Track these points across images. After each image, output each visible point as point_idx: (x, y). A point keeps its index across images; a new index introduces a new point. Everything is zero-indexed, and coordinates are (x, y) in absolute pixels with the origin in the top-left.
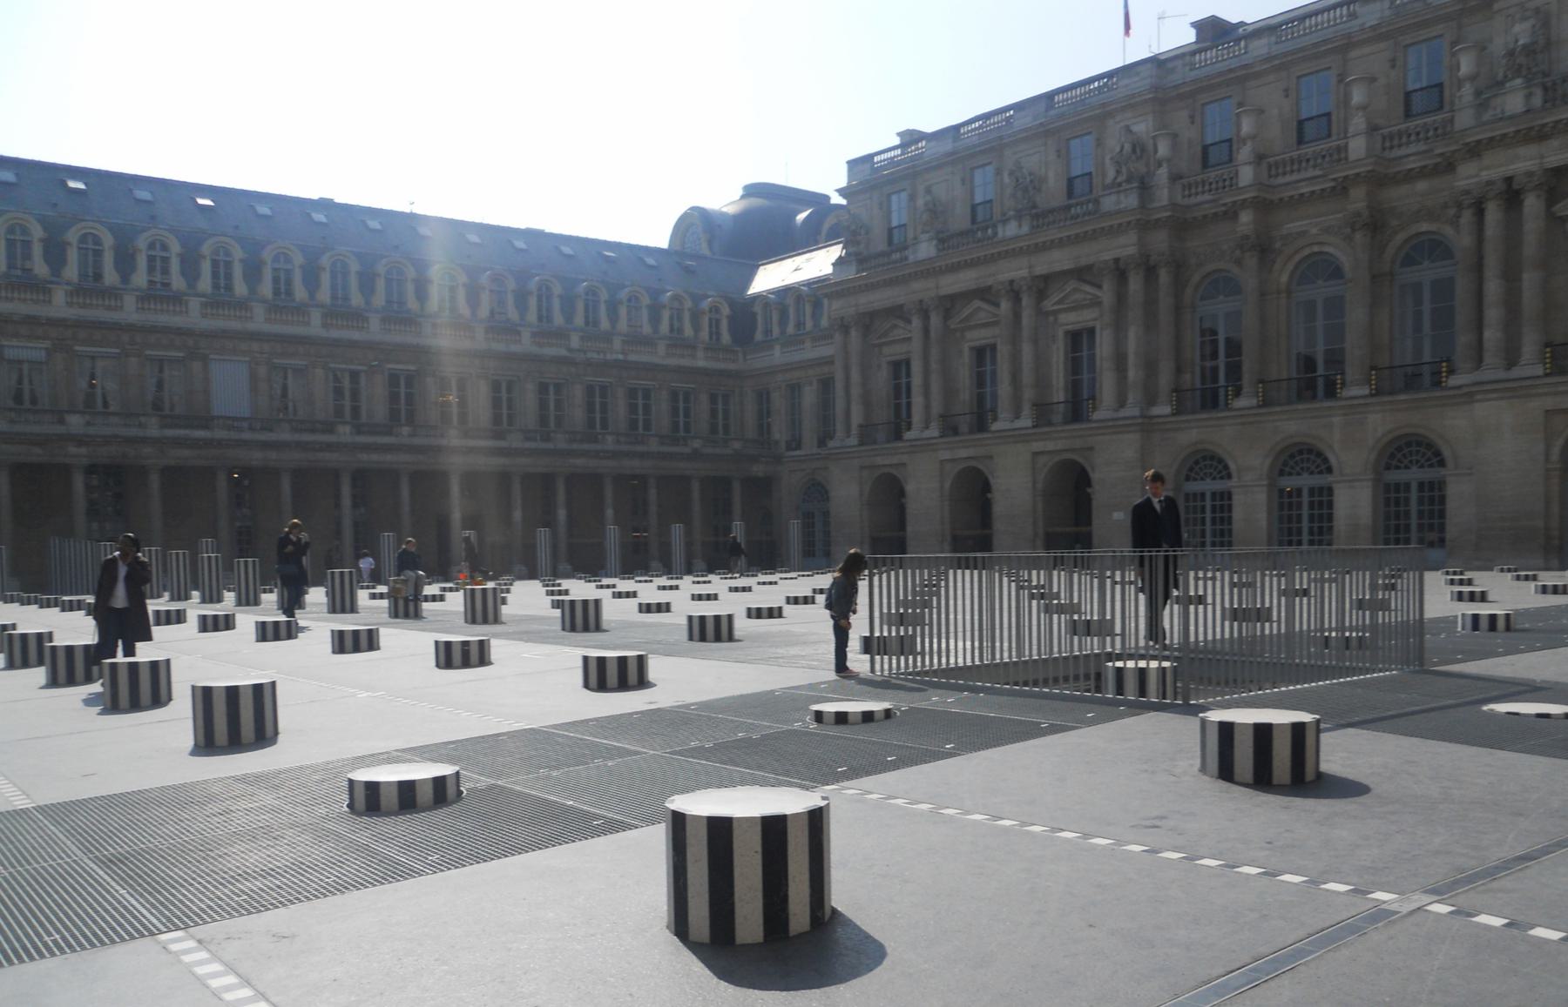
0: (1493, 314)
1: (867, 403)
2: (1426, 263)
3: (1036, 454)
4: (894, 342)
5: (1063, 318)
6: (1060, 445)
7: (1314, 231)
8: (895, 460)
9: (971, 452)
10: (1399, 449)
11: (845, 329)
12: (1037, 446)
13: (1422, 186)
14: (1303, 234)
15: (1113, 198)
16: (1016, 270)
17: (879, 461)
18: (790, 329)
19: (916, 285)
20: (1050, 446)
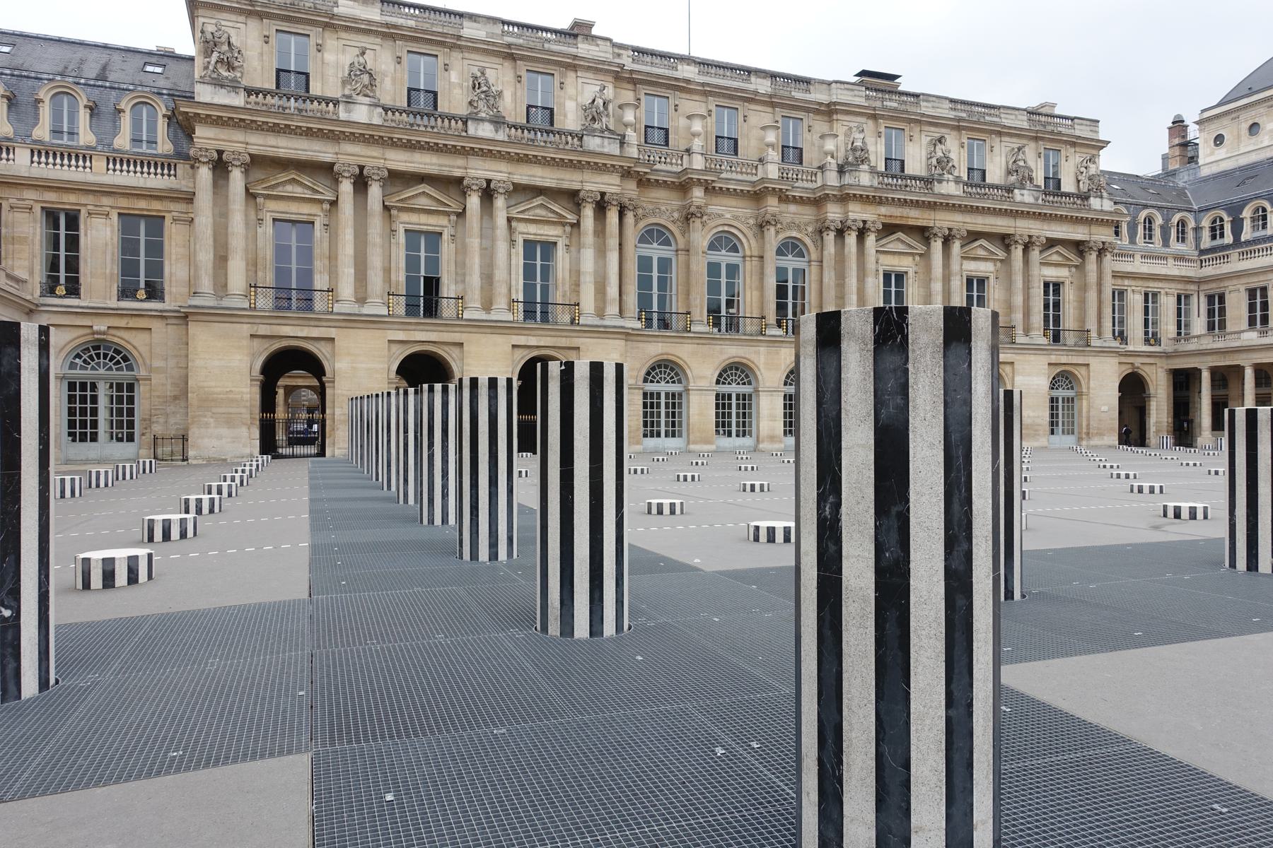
1: (253, 264)
2: (790, 257)
3: (514, 346)
5: (521, 227)
7: (728, 216)
8: (315, 333)
9: (433, 336)
11: (220, 166)
12: (522, 340)
13: (793, 208)
14: (720, 216)
15: (598, 140)
16: (499, 172)
18: (42, 132)
19: (349, 148)
20: (533, 341)
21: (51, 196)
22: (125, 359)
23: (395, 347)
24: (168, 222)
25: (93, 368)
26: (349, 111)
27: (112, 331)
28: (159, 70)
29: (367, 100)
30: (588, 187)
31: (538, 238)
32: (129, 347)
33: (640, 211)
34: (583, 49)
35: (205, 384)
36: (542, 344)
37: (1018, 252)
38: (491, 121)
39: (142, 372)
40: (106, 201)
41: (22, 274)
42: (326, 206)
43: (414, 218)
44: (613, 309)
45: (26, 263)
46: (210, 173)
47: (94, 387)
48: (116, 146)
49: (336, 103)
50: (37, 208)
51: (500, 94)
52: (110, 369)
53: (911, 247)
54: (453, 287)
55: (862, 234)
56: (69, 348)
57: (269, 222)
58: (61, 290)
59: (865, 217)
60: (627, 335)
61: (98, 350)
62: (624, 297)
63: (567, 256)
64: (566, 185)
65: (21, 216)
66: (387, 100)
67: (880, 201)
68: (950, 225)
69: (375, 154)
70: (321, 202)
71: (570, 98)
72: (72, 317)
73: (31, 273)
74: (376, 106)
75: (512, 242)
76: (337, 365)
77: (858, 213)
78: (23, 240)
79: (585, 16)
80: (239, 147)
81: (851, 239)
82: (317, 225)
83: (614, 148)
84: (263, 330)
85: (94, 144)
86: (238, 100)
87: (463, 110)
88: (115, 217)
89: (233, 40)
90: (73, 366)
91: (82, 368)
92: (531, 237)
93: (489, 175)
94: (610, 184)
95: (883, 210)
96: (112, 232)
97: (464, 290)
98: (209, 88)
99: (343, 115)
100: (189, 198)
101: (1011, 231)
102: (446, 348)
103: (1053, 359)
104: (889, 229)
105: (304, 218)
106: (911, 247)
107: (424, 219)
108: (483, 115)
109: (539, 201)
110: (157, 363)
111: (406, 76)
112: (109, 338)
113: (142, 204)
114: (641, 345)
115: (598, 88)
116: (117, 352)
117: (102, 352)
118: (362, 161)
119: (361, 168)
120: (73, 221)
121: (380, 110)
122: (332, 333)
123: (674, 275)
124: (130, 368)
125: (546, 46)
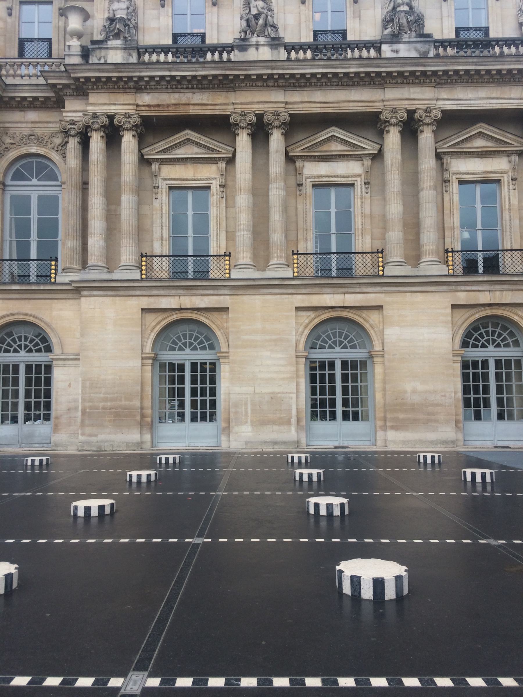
0: (97, 225)
10: (476, 329)
37: (393, 138)
53: (213, 150)
55: (113, 134)
59: (112, 110)
67: (137, 86)
68: (258, 108)
77: (103, 104)
81: (97, 143)
95: (146, 98)
101: (376, 107)
103: (462, 297)
104: (154, 128)
106: (213, 150)
123: (8, 216)
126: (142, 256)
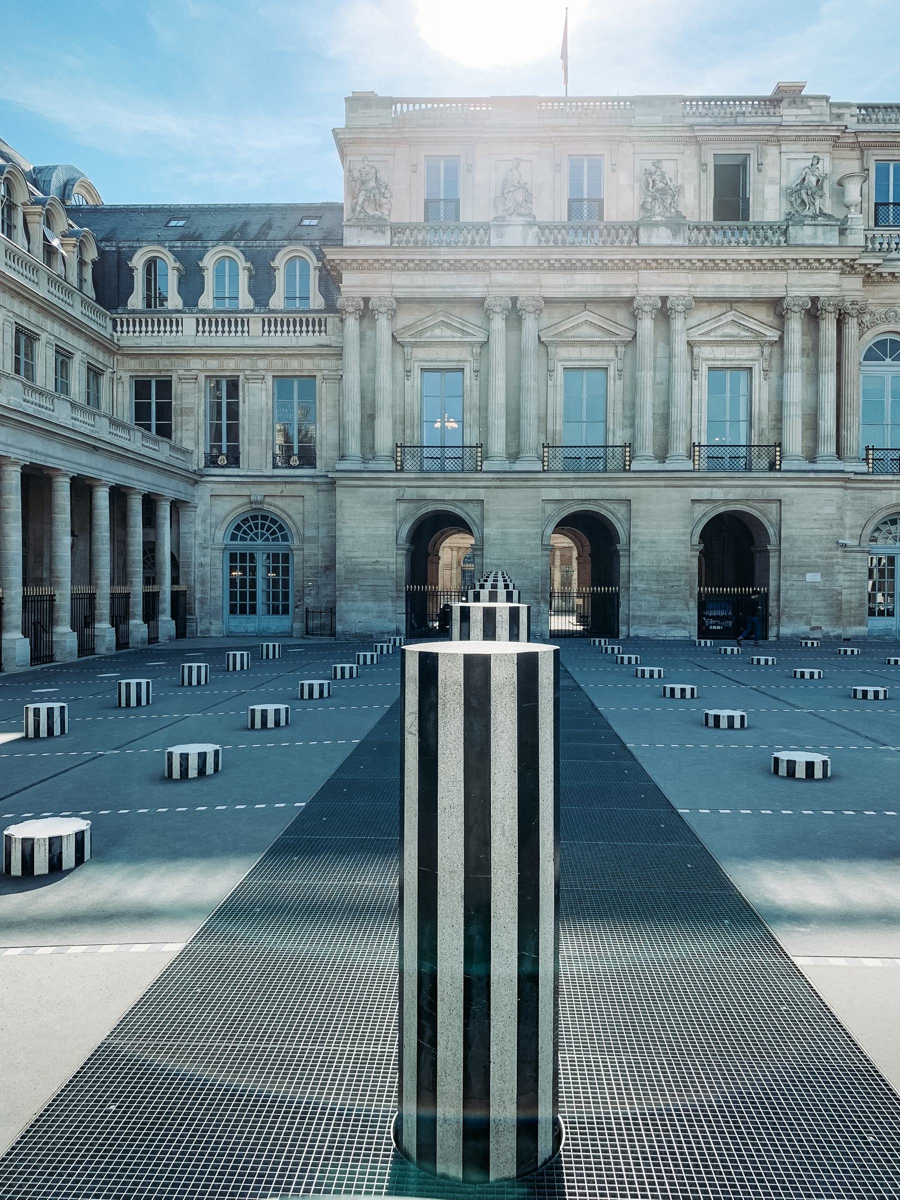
3: (694, 501)
4: (429, 344)
5: (705, 352)
6: (733, 494)
8: (463, 494)
9: (594, 494)
12: (705, 494)
15: (808, 230)
17: (433, 493)
19: (500, 277)
20: (718, 494)
21: (213, 364)
22: (281, 528)
23: (550, 508)
24: (318, 381)
25: (252, 539)
26: (500, 236)
27: (267, 500)
28: (314, 222)
29: (521, 220)
30: (794, 292)
31: (728, 364)
32: (284, 516)
33: (867, 318)
34: (789, 114)
35: (352, 555)
36: (731, 497)
38: (666, 225)
39: (295, 543)
40: (262, 364)
41: (188, 445)
42: (477, 350)
43: (574, 353)
44: (828, 448)
45: (192, 434)
46: (357, 323)
47: (252, 556)
48: (271, 307)
49: (486, 227)
50: (202, 378)
51: (680, 190)
52: (267, 539)
54: (619, 433)
56: (230, 518)
57: (417, 372)
58: (222, 460)
60: (846, 481)
61: (257, 522)
62: (844, 433)
63: (765, 384)
64: (765, 293)
65: (188, 387)
66: (543, 216)
69: (530, 282)
70: (471, 344)
71: (772, 182)
72: (233, 486)
73: (197, 444)
74: (530, 225)
75: (694, 372)
76: (486, 531)
78: (190, 411)
79: (788, 78)
80: (385, 292)
82: (467, 371)
83: (833, 238)
84: (410, 493)
85: (251, 307)
86: (384, 240)
87: (634, 215)
88: (270, 381)
89: (382, 176)
90: (234, 537)
91: (242, 539)
92: (719, 364)
93: (664, 291)
94: (824, 284)
96: (267, 396)
97: (633, 436)
98: (354, 231)
99: (494, 241)
100: (339, 353)
102: (611, 507)
105: (453, 365)
107: (586, 352)
108: (658, 218)
109: (729, 317)
110: (310, 533)
111: (566, 187)
112: (266, 507)
113: (294, 364)
114: (867, 494)
115: (809, 163)
116: (274, 522)
117: (260, 521)
118: (514, 292)
119: (514, 300)
120: (233, 386)
121: (536, 229)
122: (481, 494)
124: (285, 538)
125: (740, 120)
126: (397, 447)
